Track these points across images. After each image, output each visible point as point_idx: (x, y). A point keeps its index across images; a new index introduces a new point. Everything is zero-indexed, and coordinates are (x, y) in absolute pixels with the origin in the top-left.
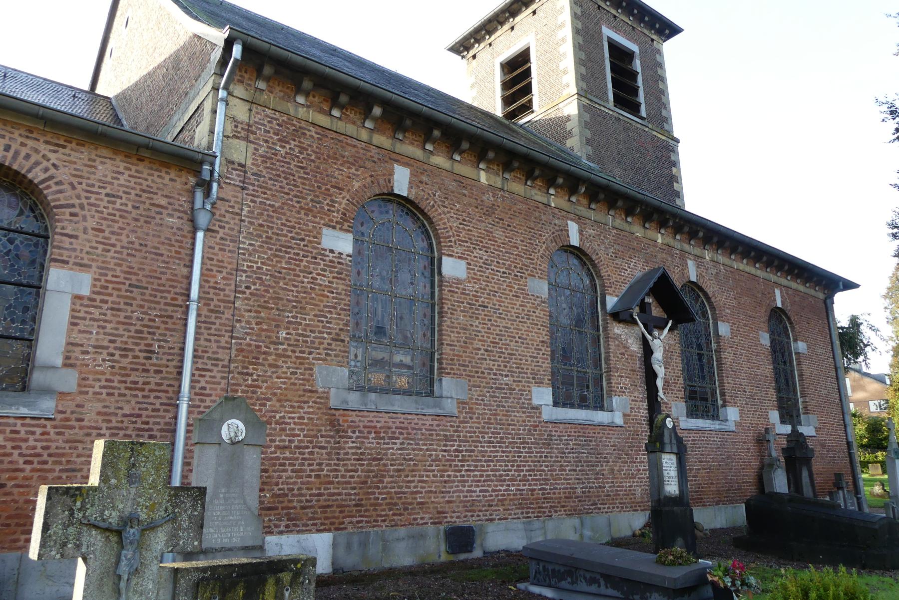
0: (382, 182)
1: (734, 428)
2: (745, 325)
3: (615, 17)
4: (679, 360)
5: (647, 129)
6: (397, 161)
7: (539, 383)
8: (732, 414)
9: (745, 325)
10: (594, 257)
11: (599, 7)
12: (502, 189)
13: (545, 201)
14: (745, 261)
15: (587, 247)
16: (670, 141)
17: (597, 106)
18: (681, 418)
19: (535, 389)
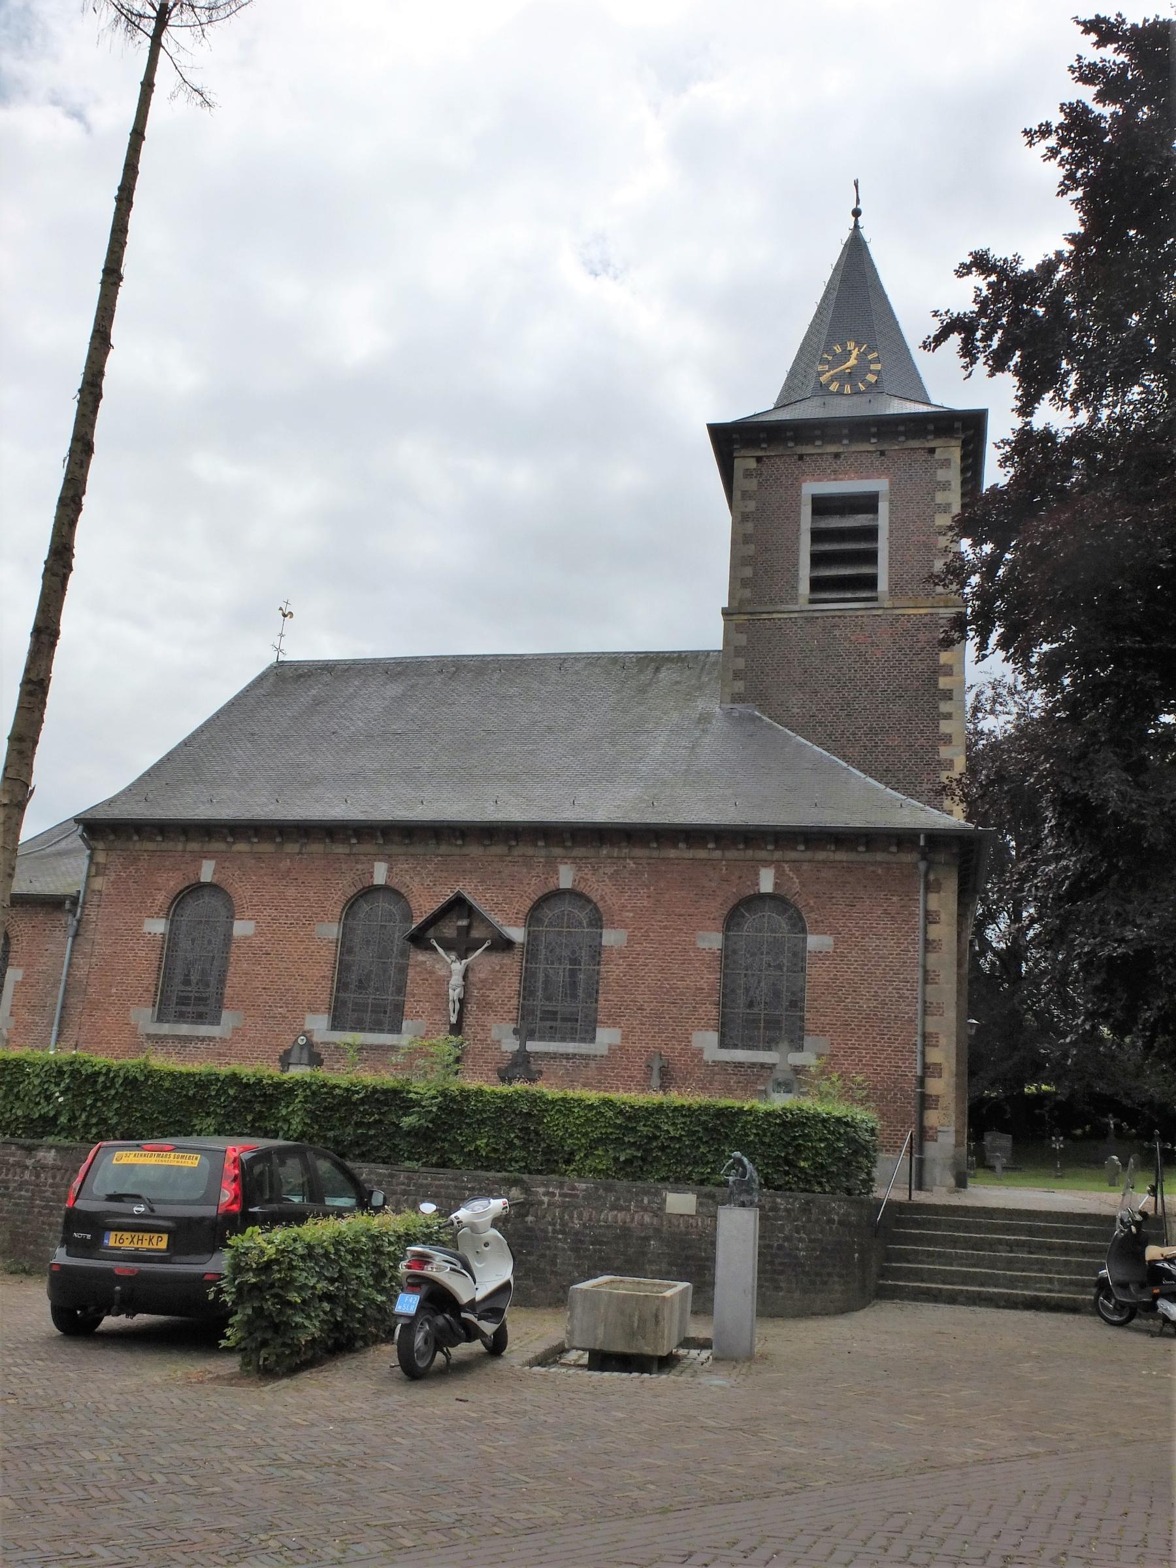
0: (191, 875)
1: (606, 1053)
2: (666, 927)
3: (837, 456)
4: (516, 980)
5: (880, 612)
6: (205, 857)
7: (314, 1011)
8: (607, 1037)
9: (666, 927)
10: (403, 891)
11: (801, 457)
12: (300, 853)
13: (347, 851)
14: (681, 845)
15: (395, 883)
16: (941, 611)
17: (765, 616)
18: (504, 1041)
19: (309, 1017)
